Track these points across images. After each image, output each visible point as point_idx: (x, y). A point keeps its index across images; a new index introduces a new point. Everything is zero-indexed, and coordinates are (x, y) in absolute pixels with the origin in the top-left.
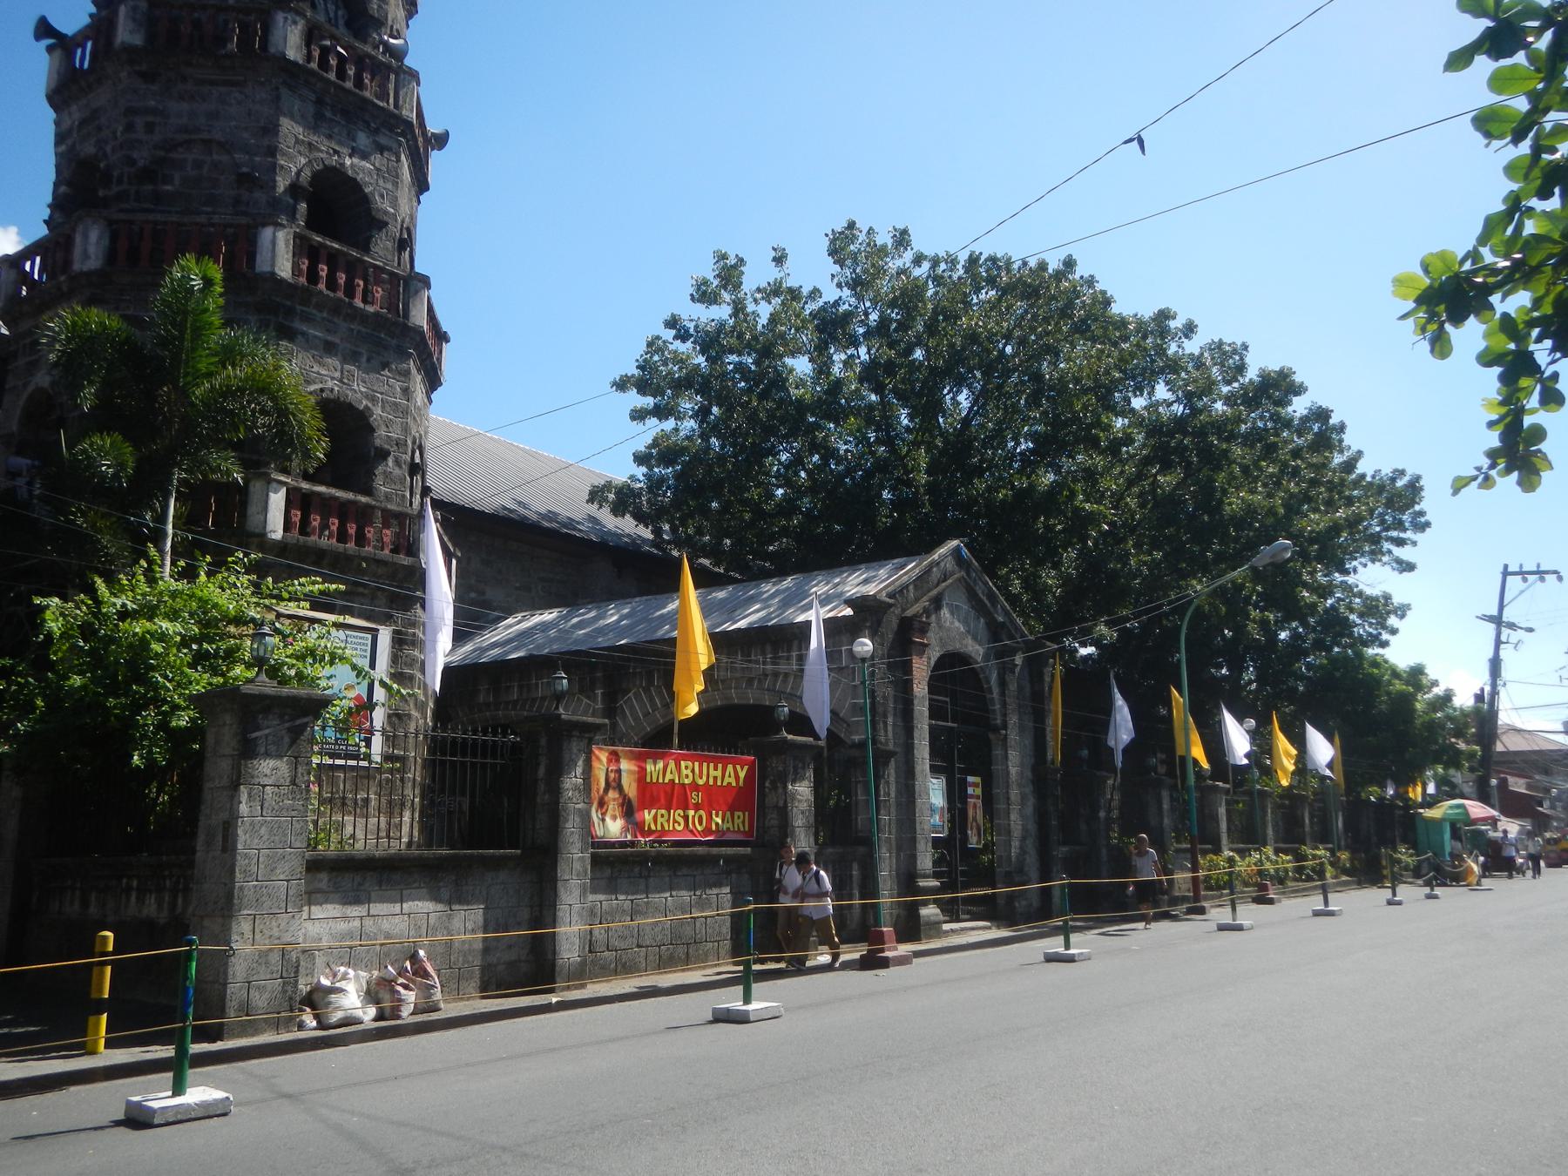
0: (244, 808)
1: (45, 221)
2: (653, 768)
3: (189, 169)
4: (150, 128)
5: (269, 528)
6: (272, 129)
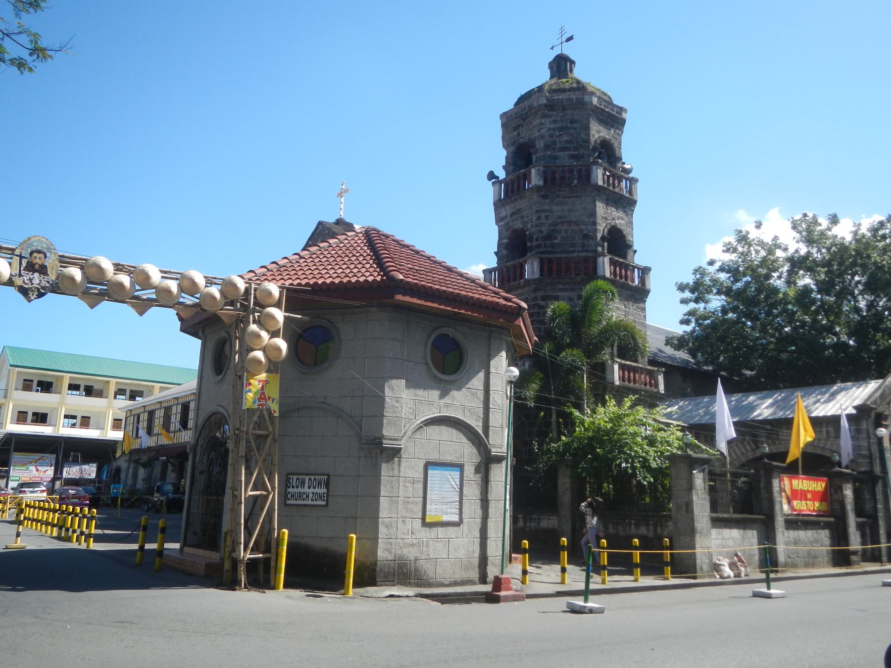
0: (694, 498)
1: (495, 253)
2: (795, 482)
3: (563, 233)
4: (547, 217)
5: (615, 381)
6: (593, 214)
